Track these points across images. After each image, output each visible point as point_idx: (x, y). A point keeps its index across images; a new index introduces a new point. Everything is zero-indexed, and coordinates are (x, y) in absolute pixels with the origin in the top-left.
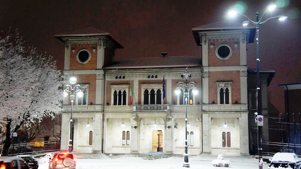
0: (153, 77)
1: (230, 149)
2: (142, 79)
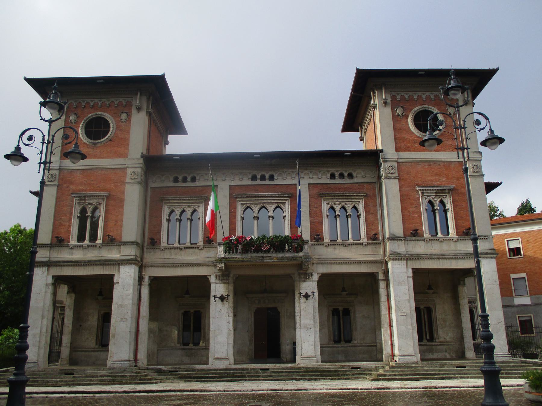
0: (263, 178)
1: (432, 345)
2: (237, 182)
